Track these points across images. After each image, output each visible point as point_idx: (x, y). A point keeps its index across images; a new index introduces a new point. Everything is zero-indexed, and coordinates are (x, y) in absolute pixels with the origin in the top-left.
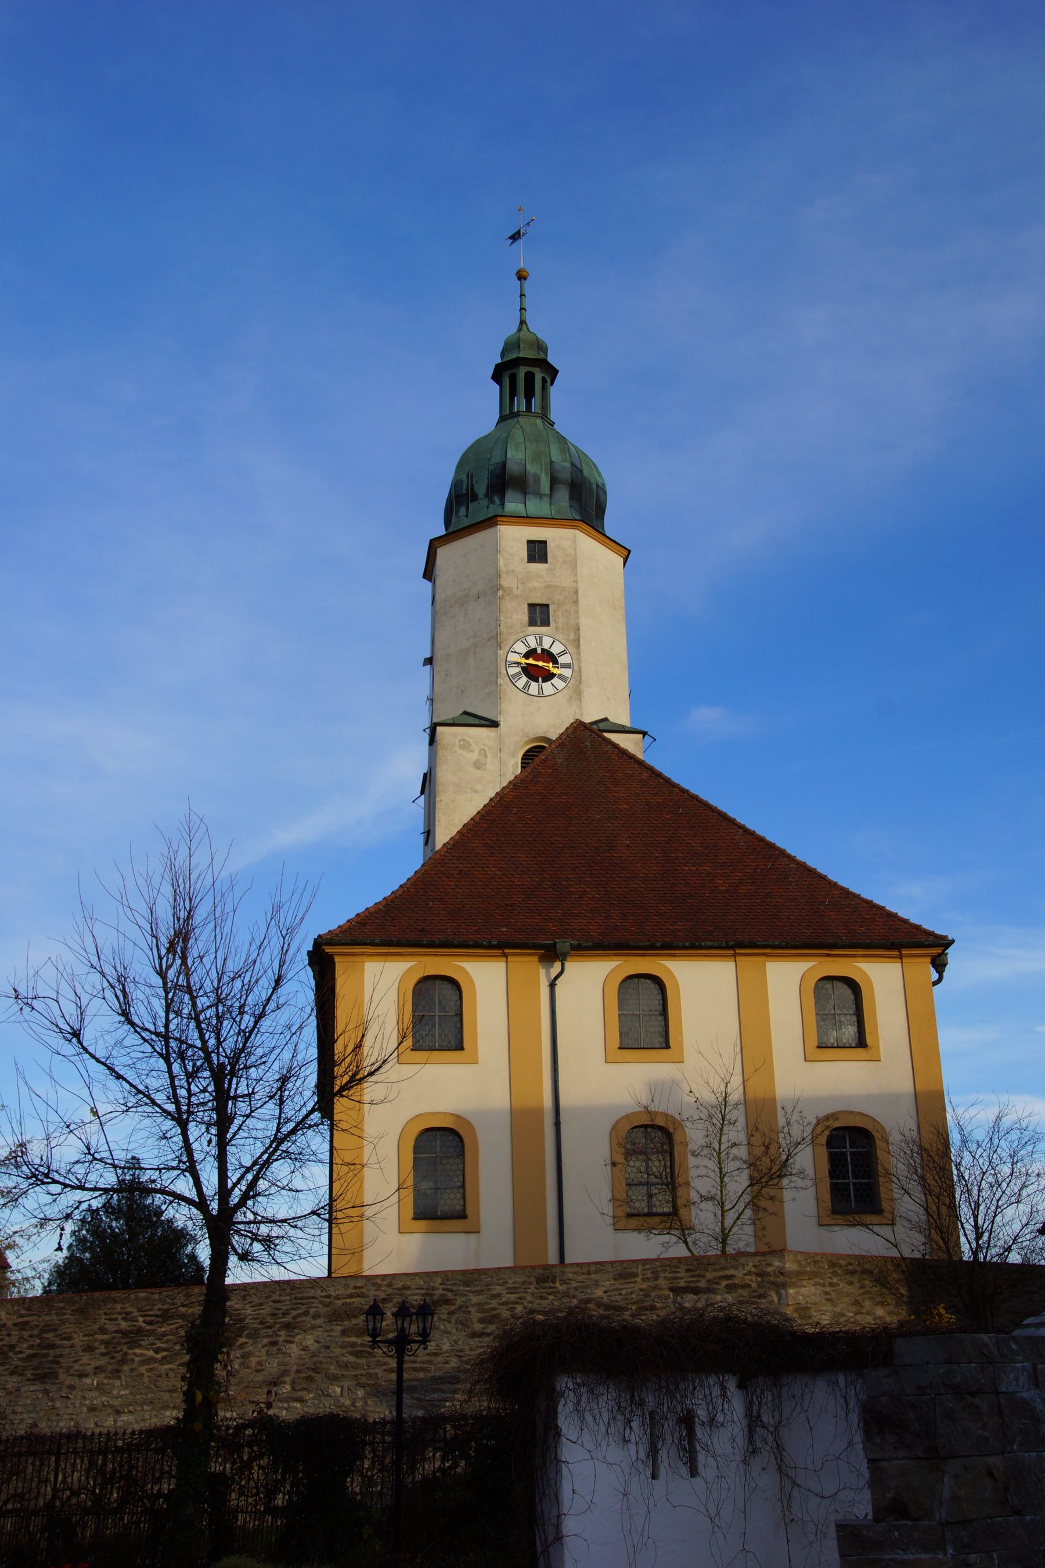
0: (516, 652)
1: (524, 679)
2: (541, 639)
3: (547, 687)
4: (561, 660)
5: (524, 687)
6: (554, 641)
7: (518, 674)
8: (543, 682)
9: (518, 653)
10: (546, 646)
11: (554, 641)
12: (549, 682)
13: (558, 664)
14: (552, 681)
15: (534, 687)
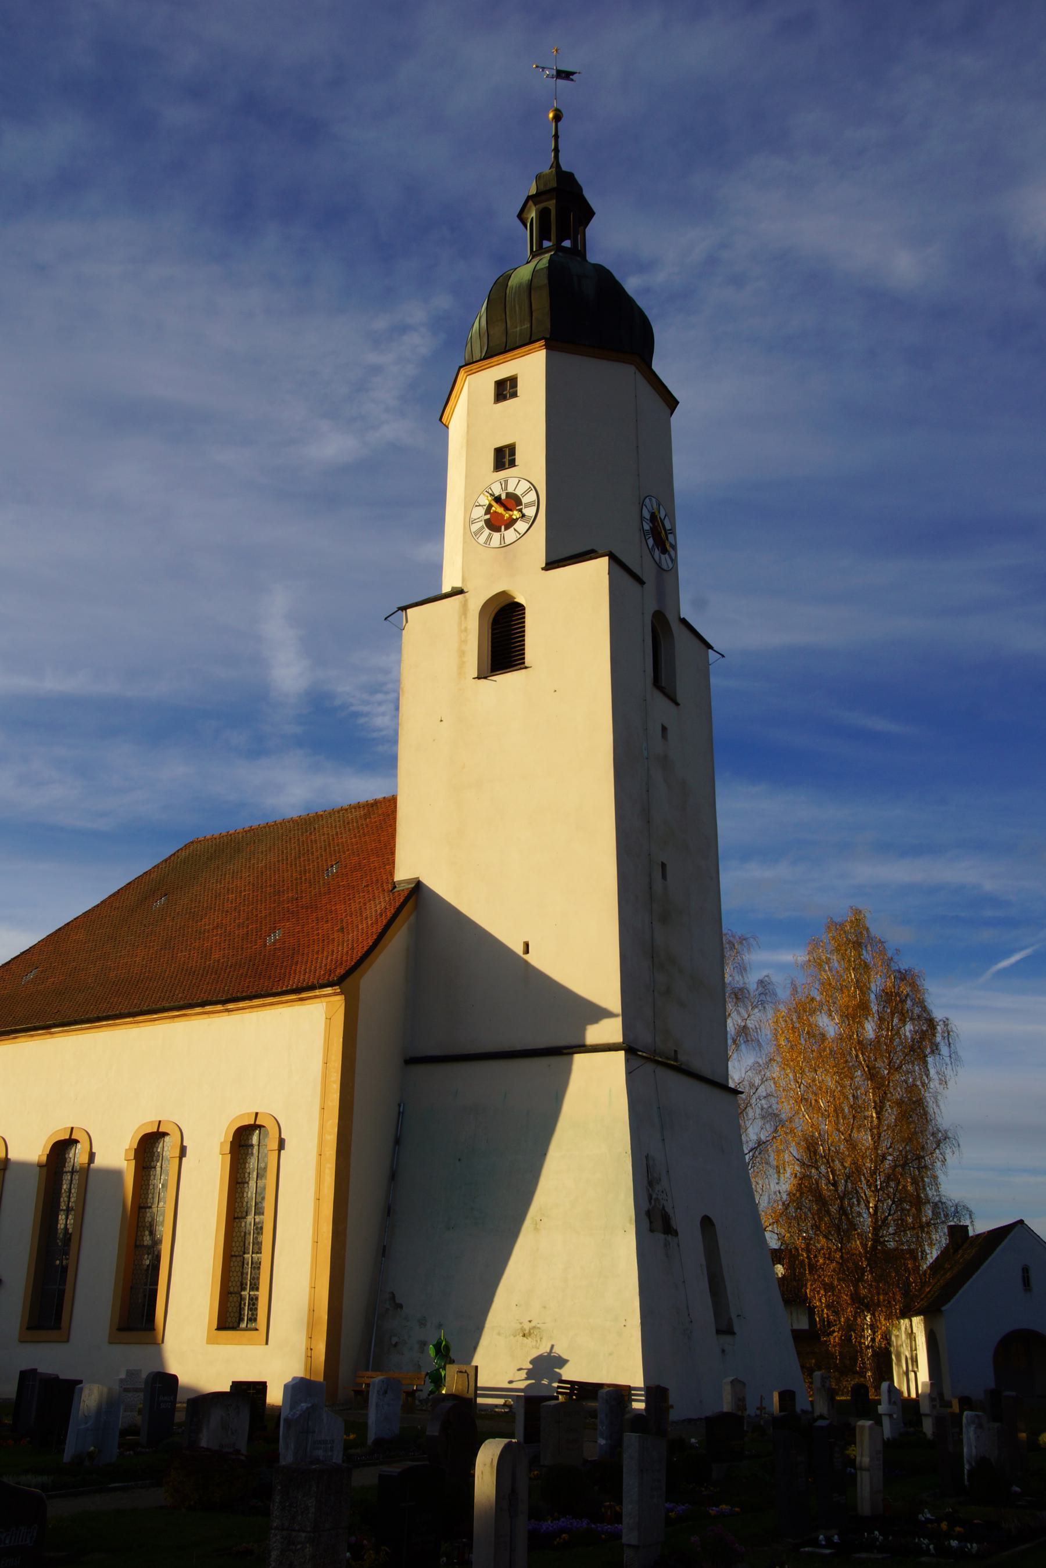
0: (480, 506)
1: (487, 531)
2: (506, 482)
3: (510, 535)
4: (524, 500)
5: (485, 543)
6: (519, 481)
7: (482, 527)
8: (506, 529)
9: (482, 506)
10: (510, 490)
11: (519, 481)
12: (512, 528)
13: (521, 505)
14: (516, 526)
15: (496, 536)
